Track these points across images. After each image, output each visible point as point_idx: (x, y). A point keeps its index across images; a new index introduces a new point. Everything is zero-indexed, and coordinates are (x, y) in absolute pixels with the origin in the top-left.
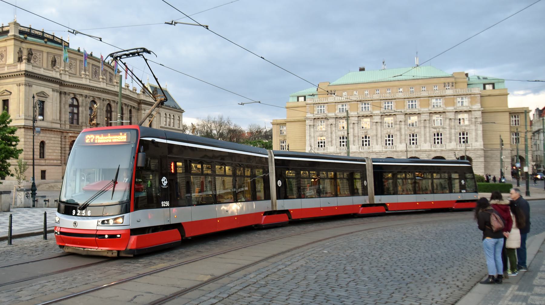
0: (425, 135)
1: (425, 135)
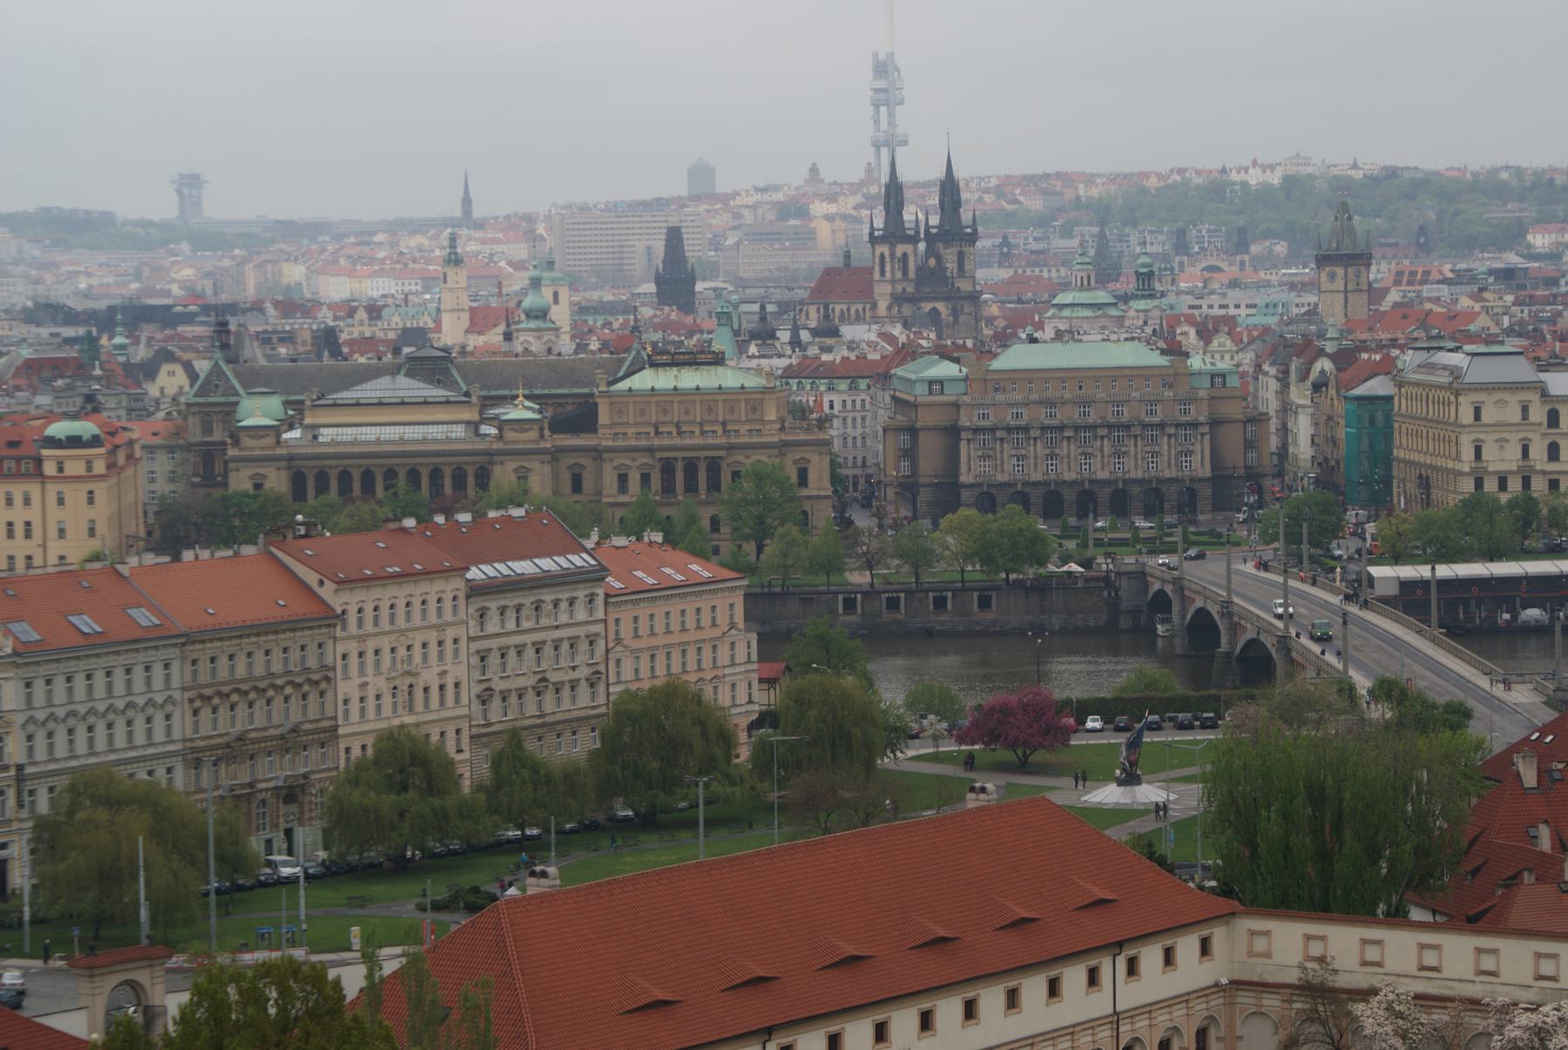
0: (1136, 456)
1: (1136, 456)
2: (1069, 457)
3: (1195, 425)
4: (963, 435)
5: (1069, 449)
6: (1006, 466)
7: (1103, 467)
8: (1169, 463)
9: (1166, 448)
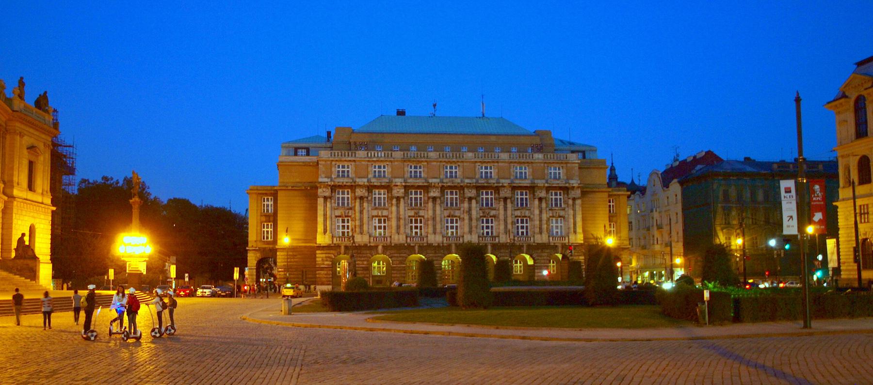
2: (434, 219)
3: (566, 189)
4: (322, 192)
5: (434, 211)
6: (365, 228)
7: (470, 232)
8: (541, 228)
9: (537, 212)
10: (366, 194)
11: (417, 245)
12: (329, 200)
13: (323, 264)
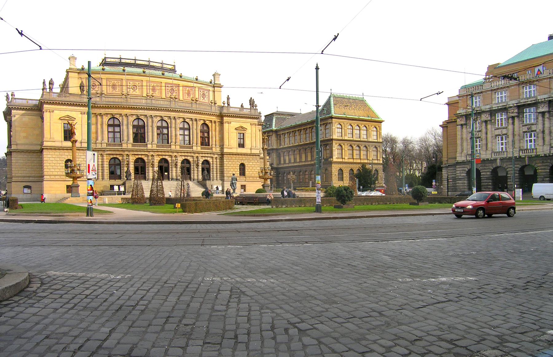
2: (543, 132)
5: (544, 124)
6: (489, 145)
10: (489, 119)
11: (526, 156)
12: (464, 126)
13: (461, 176)
